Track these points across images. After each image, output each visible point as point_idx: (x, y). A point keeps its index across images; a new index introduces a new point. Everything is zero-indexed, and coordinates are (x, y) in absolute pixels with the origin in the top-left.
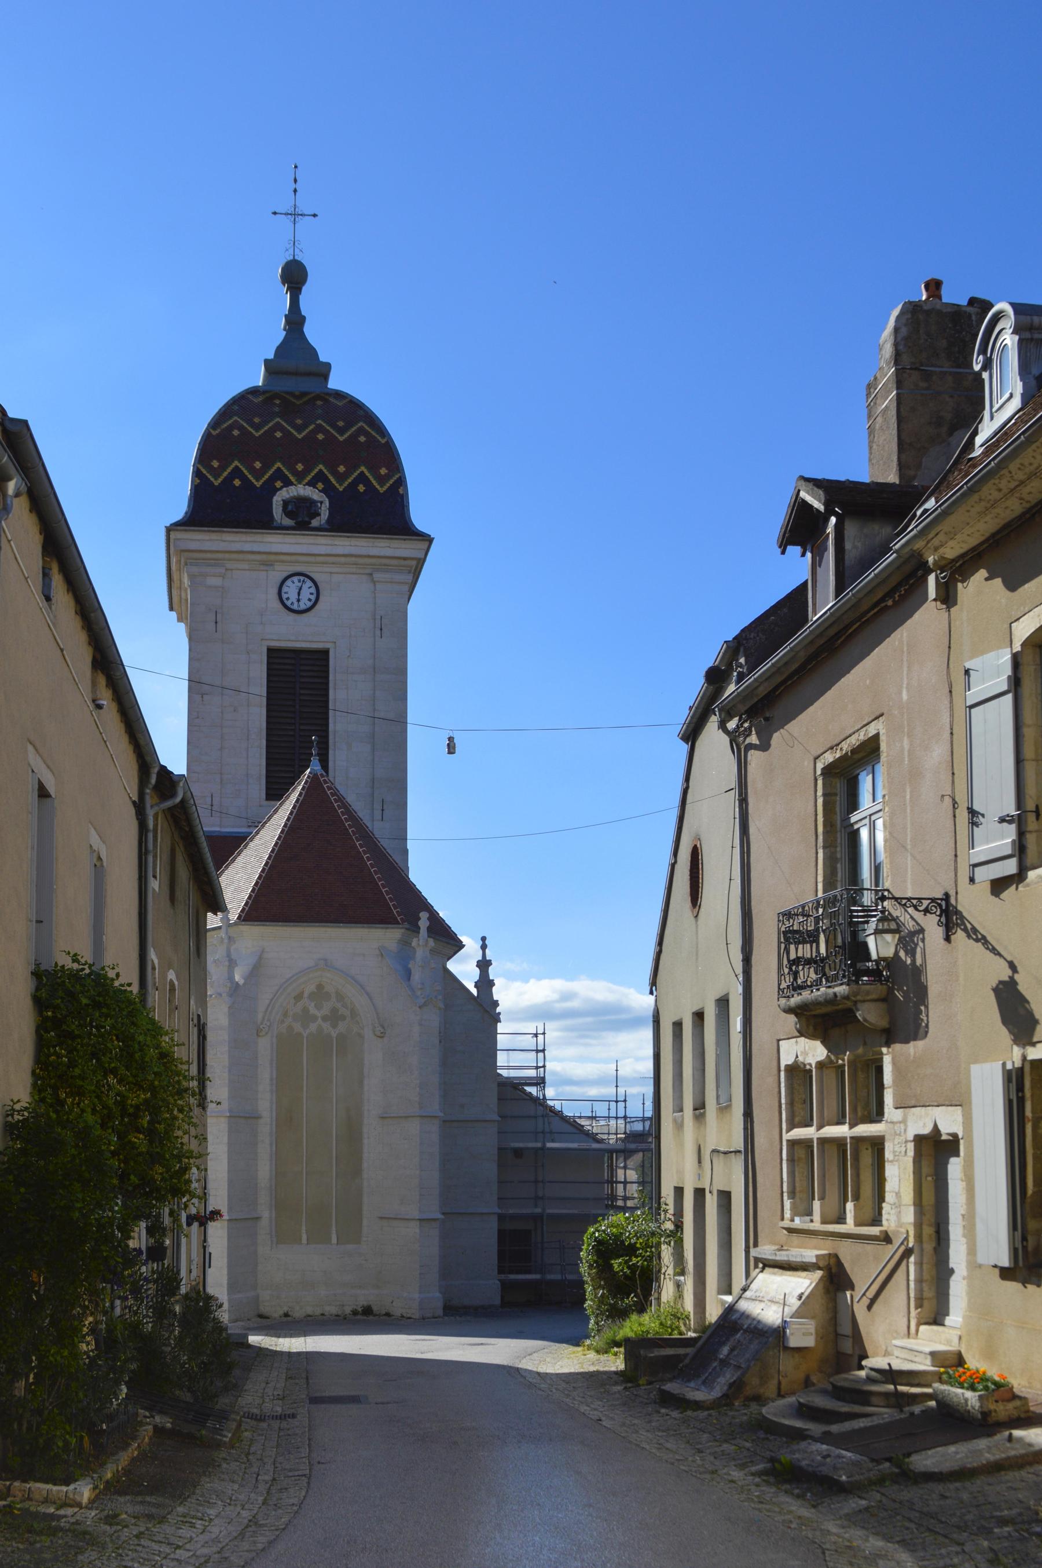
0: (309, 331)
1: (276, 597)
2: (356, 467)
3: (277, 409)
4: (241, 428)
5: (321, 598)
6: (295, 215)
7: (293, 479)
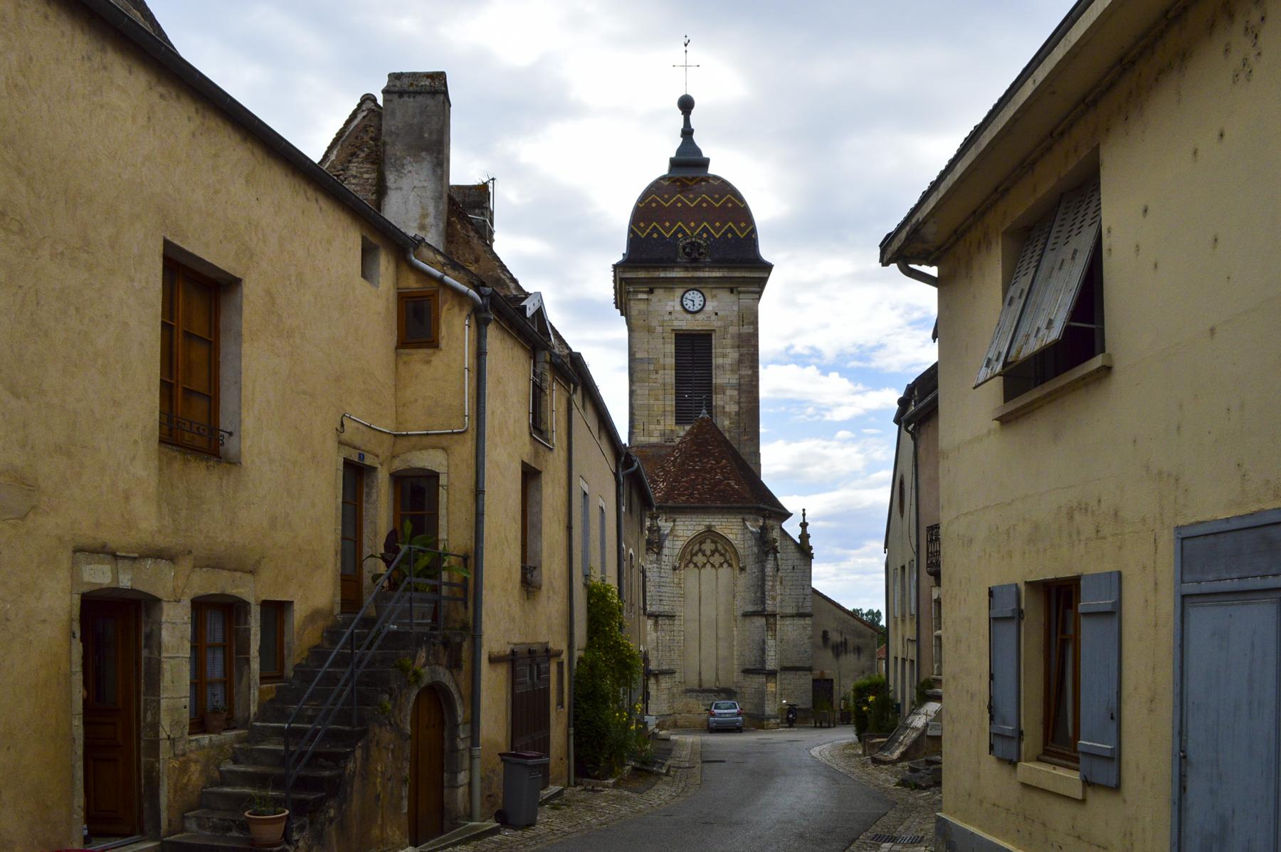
0: (696, 138)
1: (679, 304)
4: (657, 202)
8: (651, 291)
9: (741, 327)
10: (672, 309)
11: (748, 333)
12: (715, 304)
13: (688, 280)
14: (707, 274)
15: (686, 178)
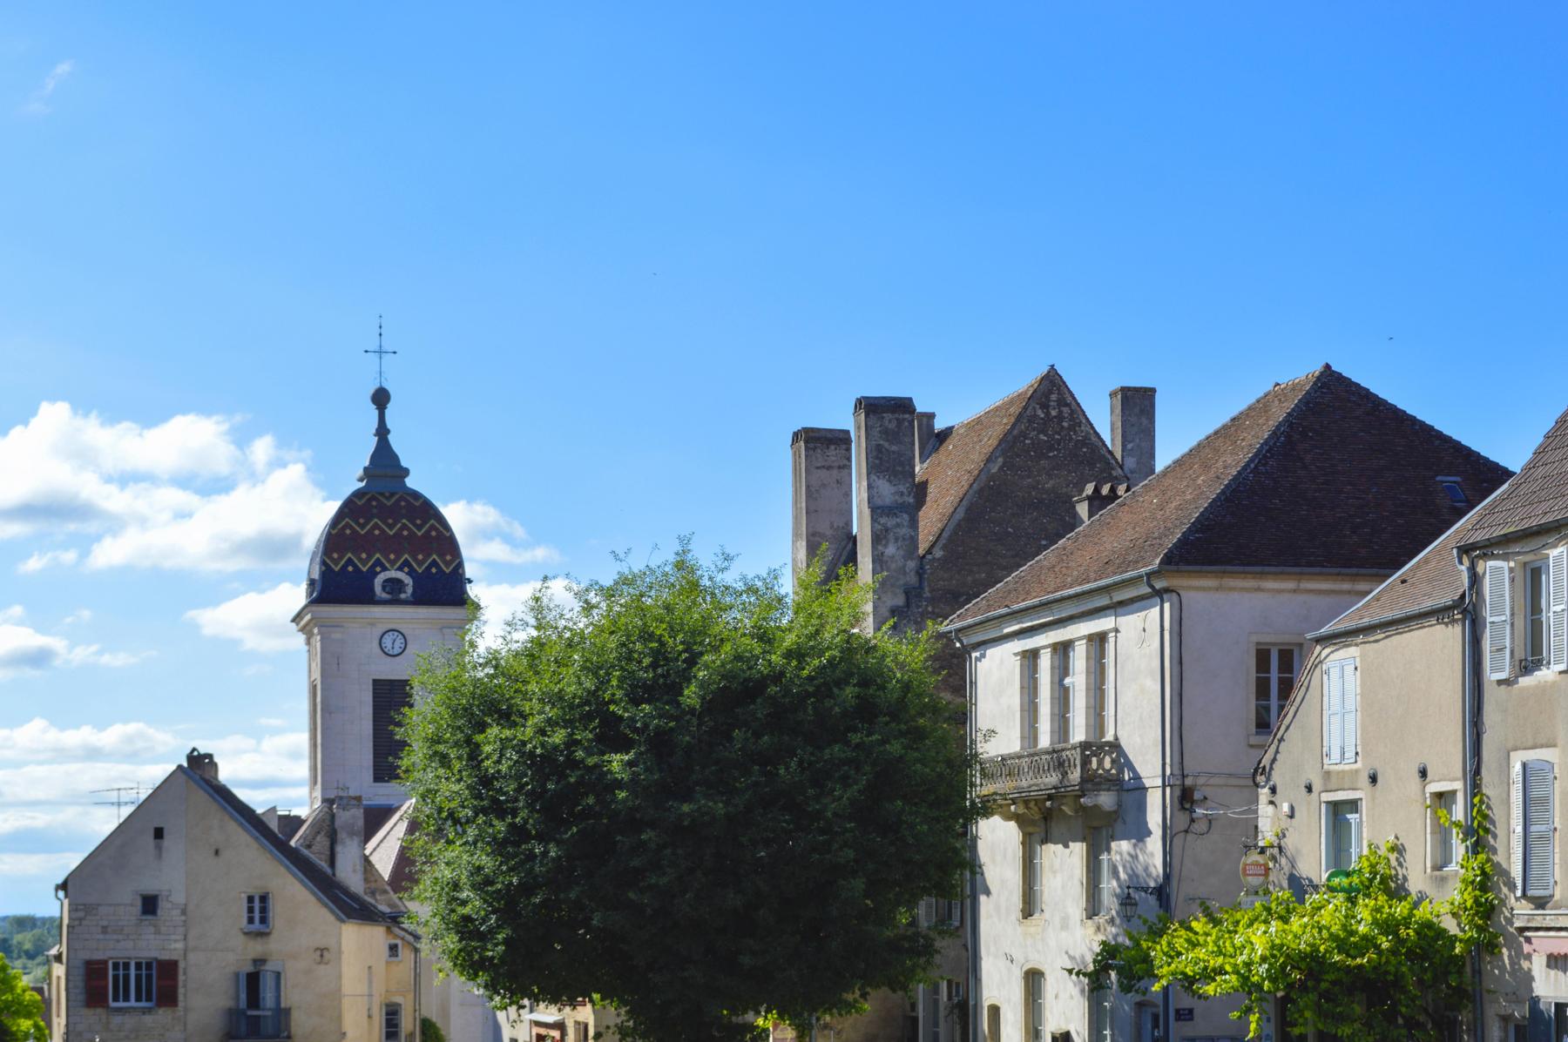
0: (392, 439)
2: (429, 555)
3: (375, 511)
6: (380, 352)
7: (387, 565)
15: (382, 494)
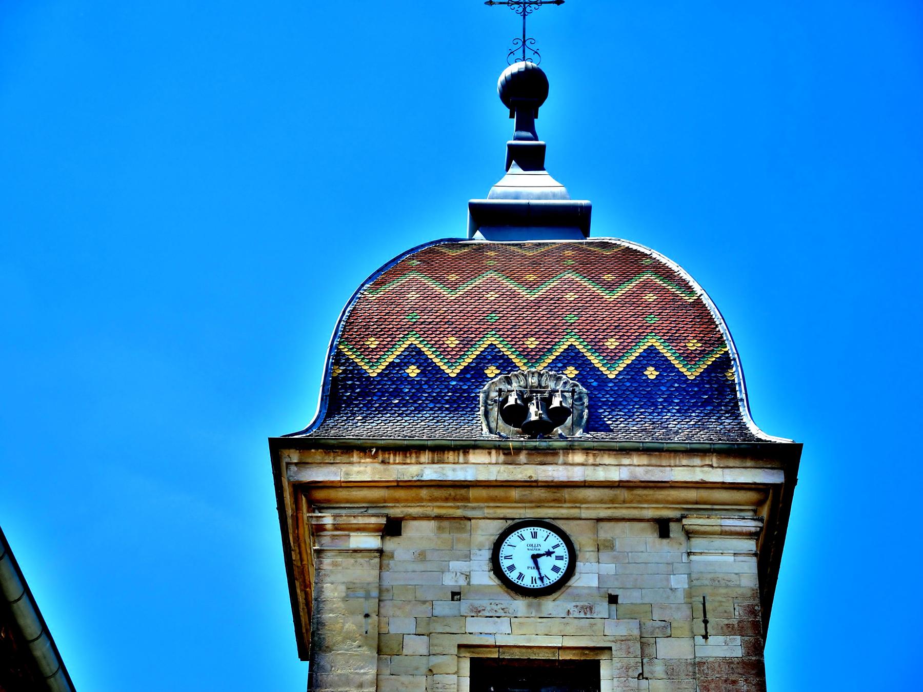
1: (486, 565)
5: (580, 565)
8: (392, 528)
9: (700, 640)
10: (462, 582)
11: (729, 662)
12: (609, 568)
13: (515, 493)
14: (577, 474)
